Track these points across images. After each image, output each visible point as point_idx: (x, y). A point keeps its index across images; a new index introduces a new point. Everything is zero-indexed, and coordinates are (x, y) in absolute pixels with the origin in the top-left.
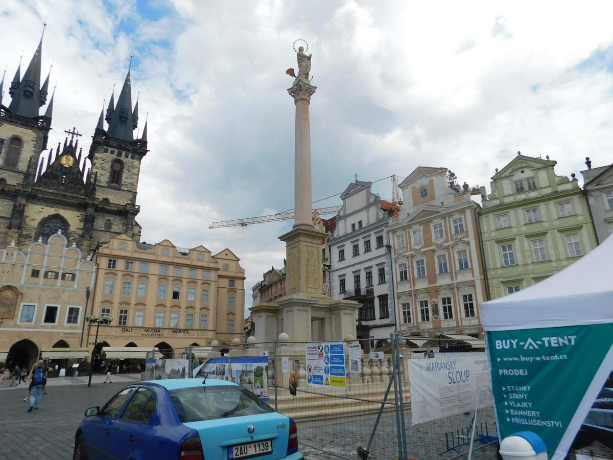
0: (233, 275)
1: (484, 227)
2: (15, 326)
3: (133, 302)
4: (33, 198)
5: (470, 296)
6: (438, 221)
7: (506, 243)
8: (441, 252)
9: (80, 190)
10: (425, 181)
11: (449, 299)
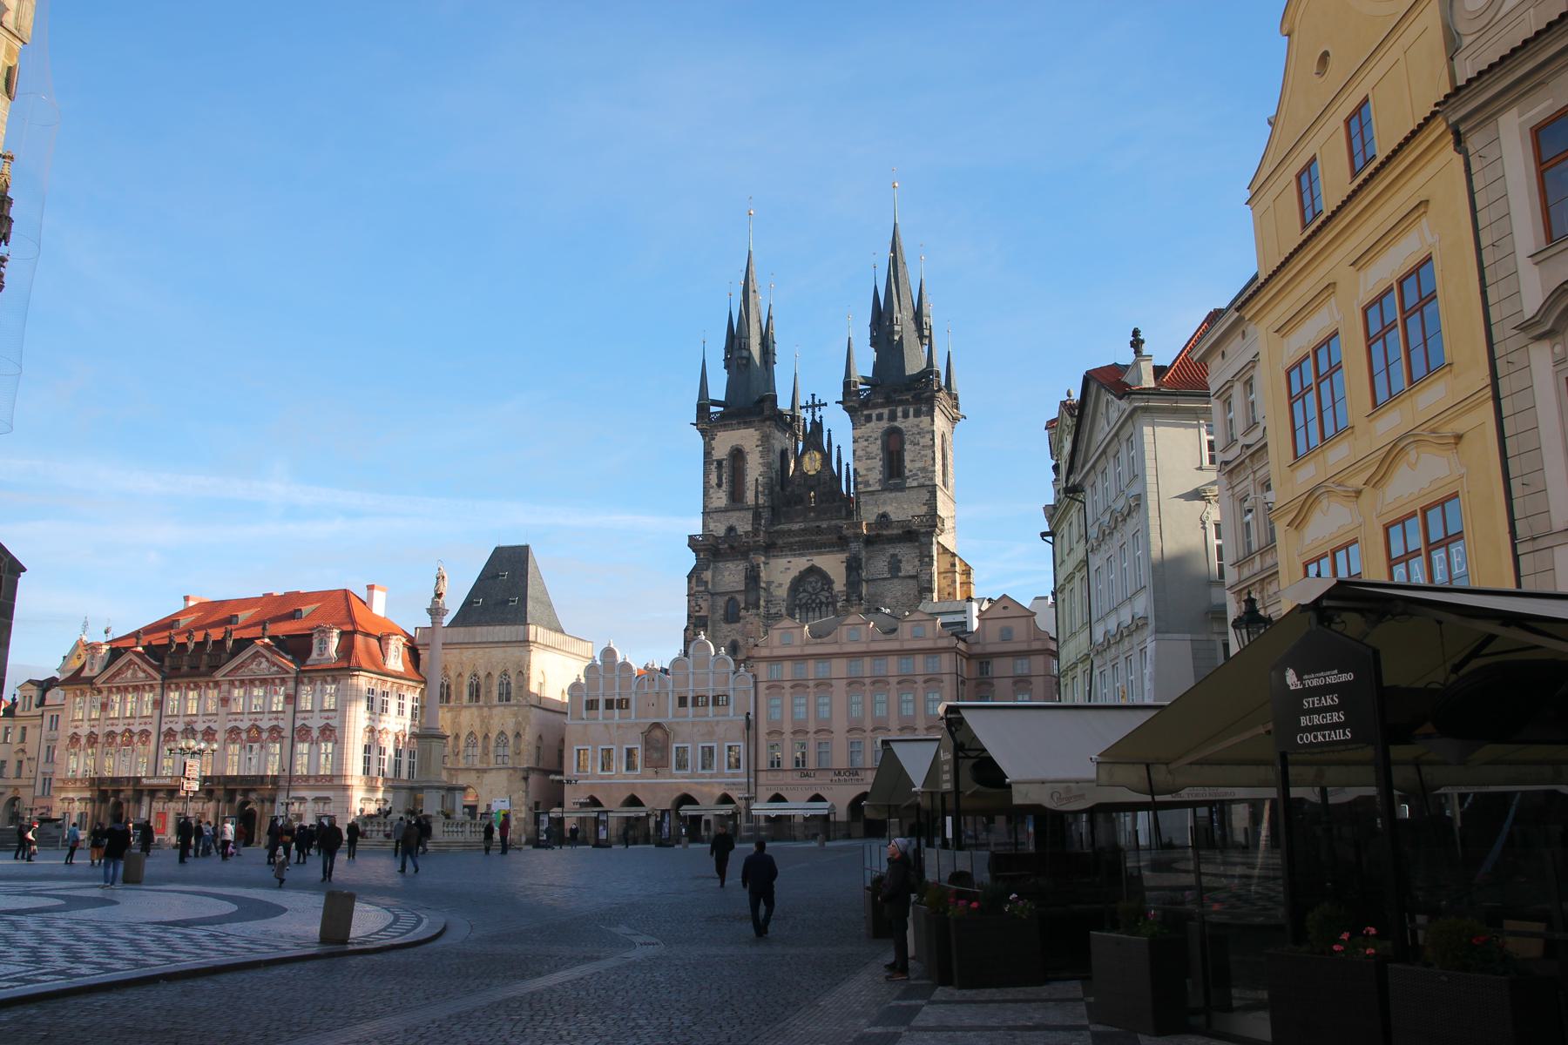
0: (1024, 647)
2: (672, 776)
3: (812, 727)
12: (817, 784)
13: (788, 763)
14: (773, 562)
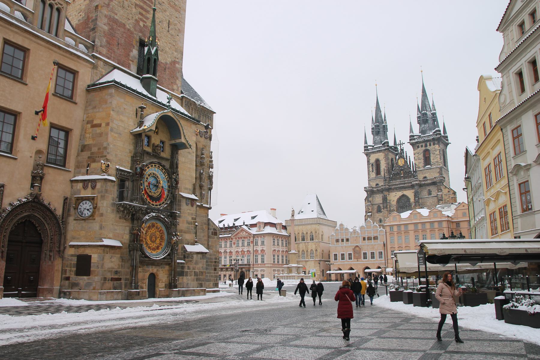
2: (362, 261)
4: (389, 190)
14: (391, 194)
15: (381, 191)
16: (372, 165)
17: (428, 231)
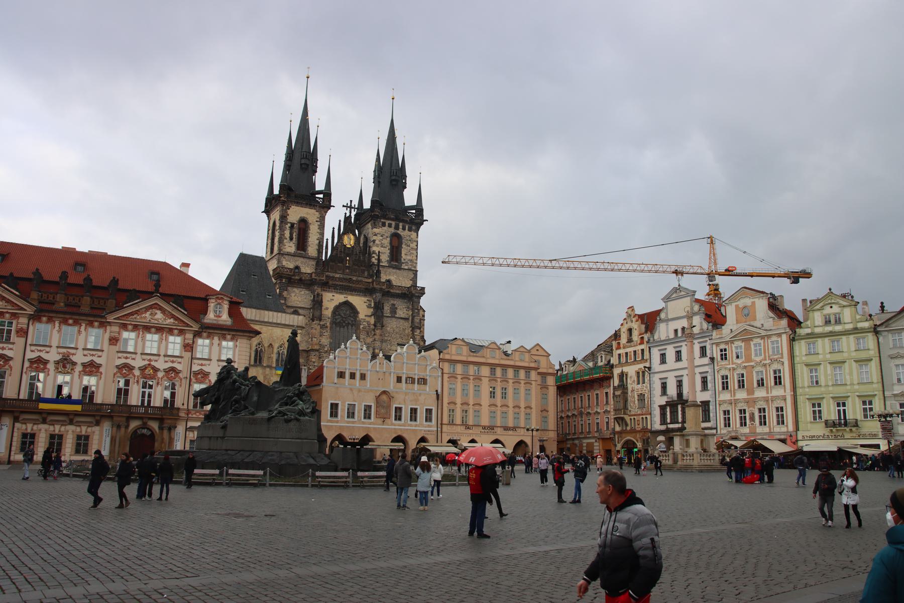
1: (797, 352)
2: (392, 424)
5: (782, 408)
6: (758, 340)
7: (812, 367)
8: (758, 369)
9: (363, 272)
10: (747, 301)
11: (764, 409)
12: (474, 433)
13: (458, 420)
15: (307, 283)
16: (292, 225)
17: (511, 381)
